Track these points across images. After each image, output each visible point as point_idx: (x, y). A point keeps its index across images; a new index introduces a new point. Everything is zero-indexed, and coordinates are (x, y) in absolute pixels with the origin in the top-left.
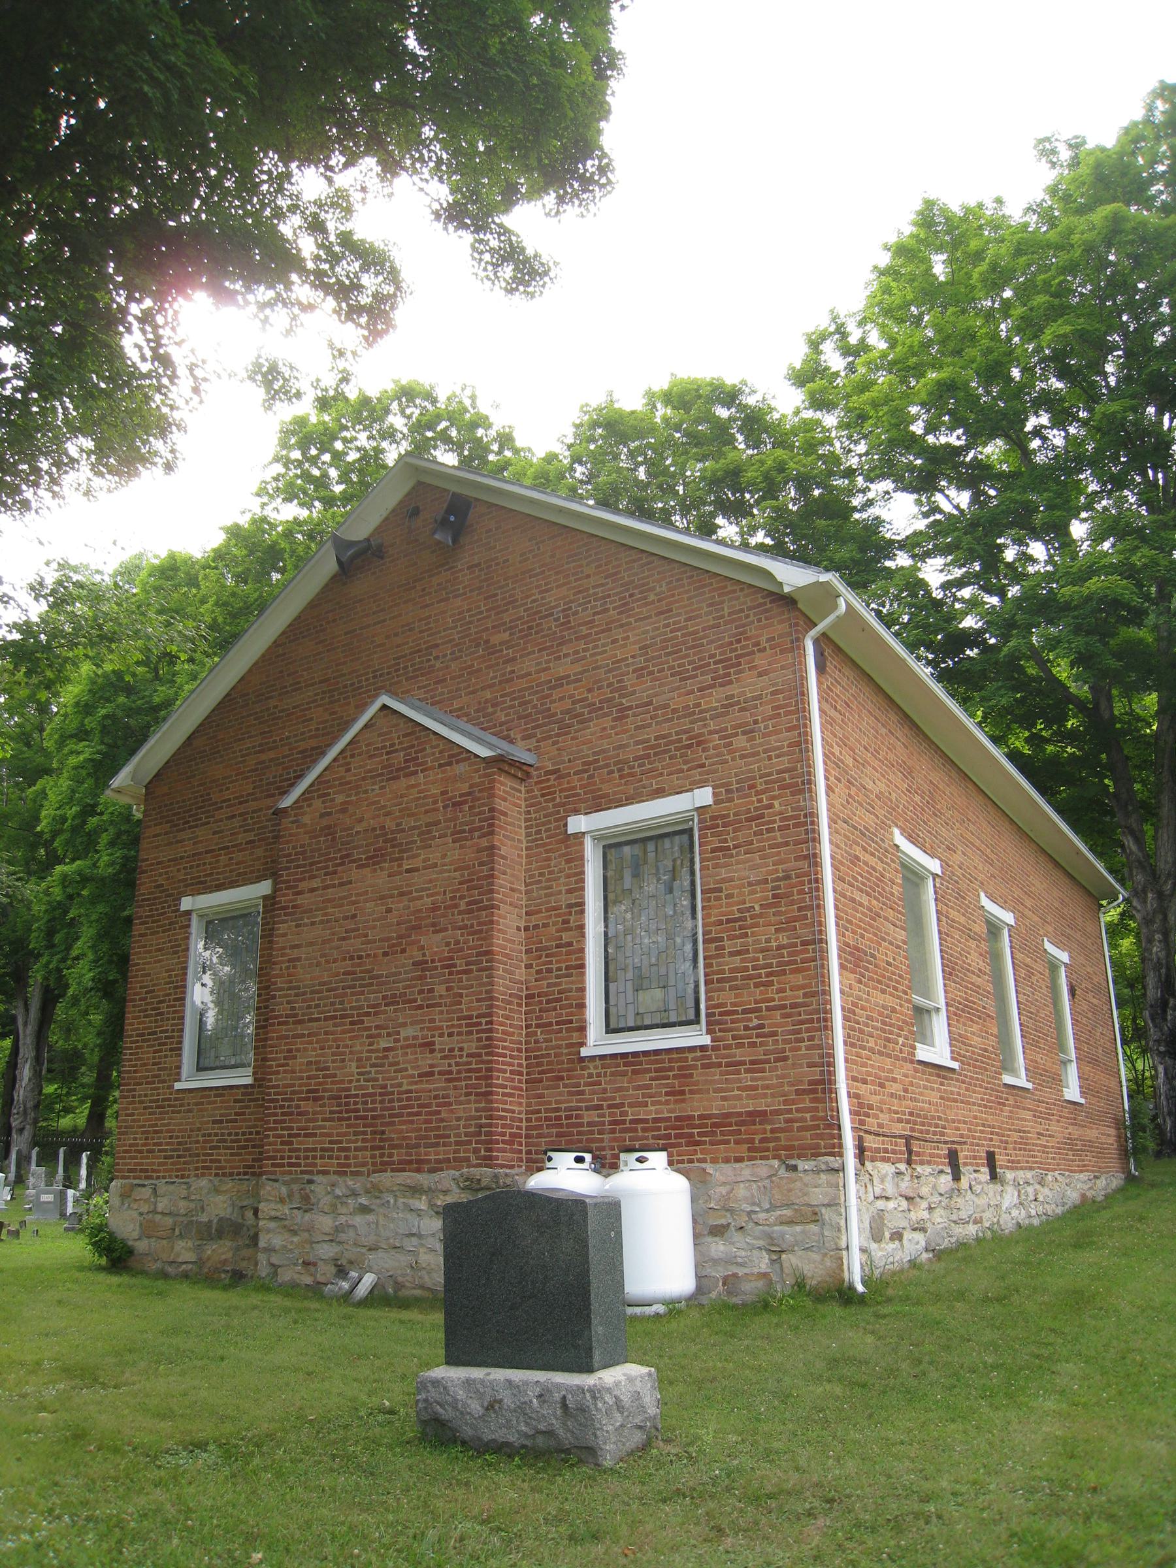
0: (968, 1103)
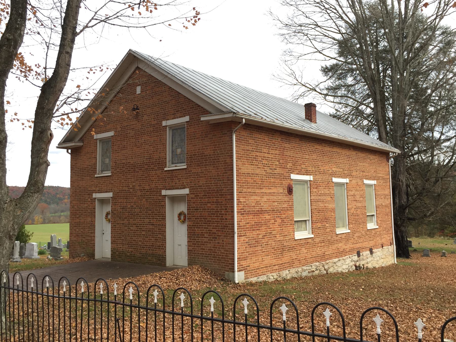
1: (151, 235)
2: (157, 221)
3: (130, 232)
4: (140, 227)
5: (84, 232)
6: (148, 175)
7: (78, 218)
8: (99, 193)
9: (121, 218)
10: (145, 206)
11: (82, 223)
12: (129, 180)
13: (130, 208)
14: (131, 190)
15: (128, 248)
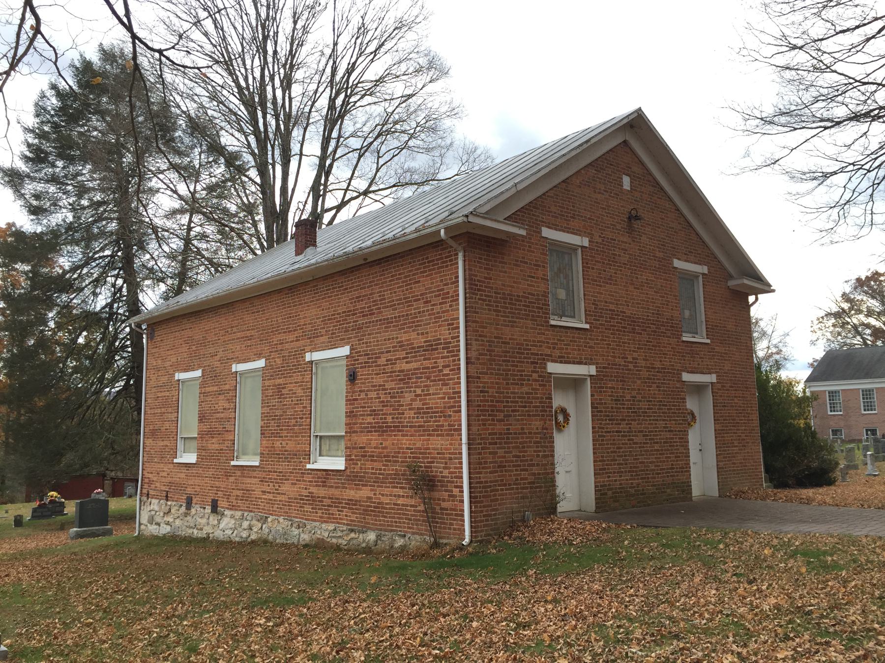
0: (202, 477)
1: (668, 450)
2: (676, 424)
3: (633, 448)
4: (650, 435)
5: (524, 456)
6: (657, 343)
7: (500, 421)
8: (561, 362)
9: (613, 420)
10: (656, 398)
11: (515, 434)
12: (624, 346)
13: (630, 400)
14: (631, 366)
15: (630, 479)
